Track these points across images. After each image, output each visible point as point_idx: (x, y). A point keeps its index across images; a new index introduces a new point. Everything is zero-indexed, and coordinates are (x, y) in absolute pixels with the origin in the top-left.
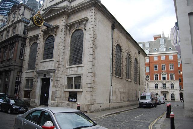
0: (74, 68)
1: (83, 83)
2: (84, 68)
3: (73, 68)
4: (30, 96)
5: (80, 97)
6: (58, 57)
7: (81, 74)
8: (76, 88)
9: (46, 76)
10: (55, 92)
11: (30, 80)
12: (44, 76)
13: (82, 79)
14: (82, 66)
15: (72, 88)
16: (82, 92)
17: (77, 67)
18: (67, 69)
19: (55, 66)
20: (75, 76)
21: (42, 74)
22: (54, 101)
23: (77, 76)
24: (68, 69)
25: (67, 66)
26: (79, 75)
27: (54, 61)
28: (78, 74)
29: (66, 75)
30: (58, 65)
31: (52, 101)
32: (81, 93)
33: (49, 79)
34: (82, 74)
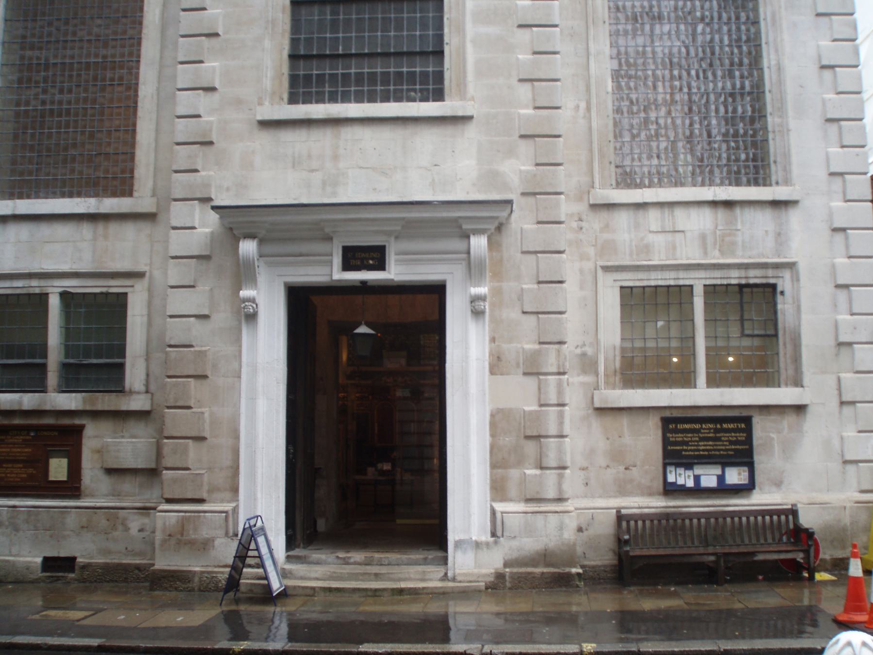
0: (694, 212)
1: (807, 340)
2: (794, 217)
3: (679, 212)
4: (75, 470)
5: (789, 448)
6: (524, 92)
7: (777, 266)
8: (713, 381)
9: (381, 266)
10: (536, 417)
11: (54, 302)
12: (347, 266)
13: (784, 306)
14: (776, 204)
15: (686, 380)
16: (800, 409)
17: (729, 204)
18: (604, 215)
19: (492, 177)
20: (717, 278)
21: (329, 239)
22: (528, 500)
23: (735, 278)
24: (622, 218)
25: (603, 186)
26: (755, 277)
27: (471, 131)
28: (739, 266)
29: (606, 269)
30: (529, 168)
31: (499, 507)
32: (790, 419)
33: (438, 291)
34: (791, 266)
